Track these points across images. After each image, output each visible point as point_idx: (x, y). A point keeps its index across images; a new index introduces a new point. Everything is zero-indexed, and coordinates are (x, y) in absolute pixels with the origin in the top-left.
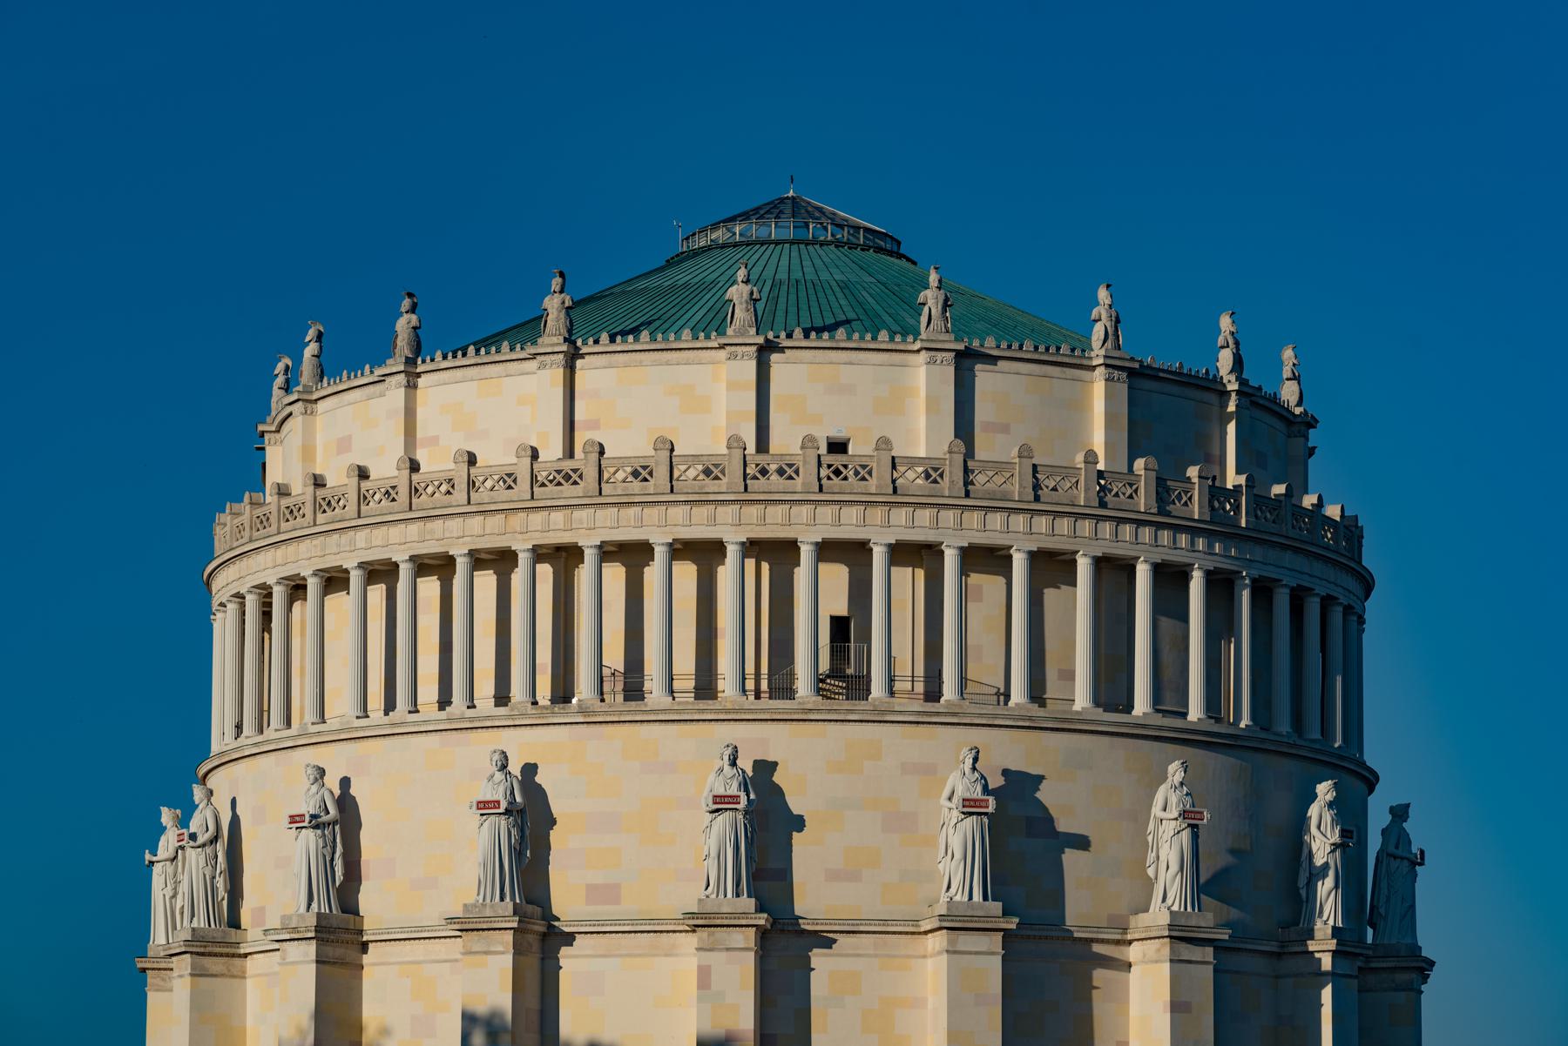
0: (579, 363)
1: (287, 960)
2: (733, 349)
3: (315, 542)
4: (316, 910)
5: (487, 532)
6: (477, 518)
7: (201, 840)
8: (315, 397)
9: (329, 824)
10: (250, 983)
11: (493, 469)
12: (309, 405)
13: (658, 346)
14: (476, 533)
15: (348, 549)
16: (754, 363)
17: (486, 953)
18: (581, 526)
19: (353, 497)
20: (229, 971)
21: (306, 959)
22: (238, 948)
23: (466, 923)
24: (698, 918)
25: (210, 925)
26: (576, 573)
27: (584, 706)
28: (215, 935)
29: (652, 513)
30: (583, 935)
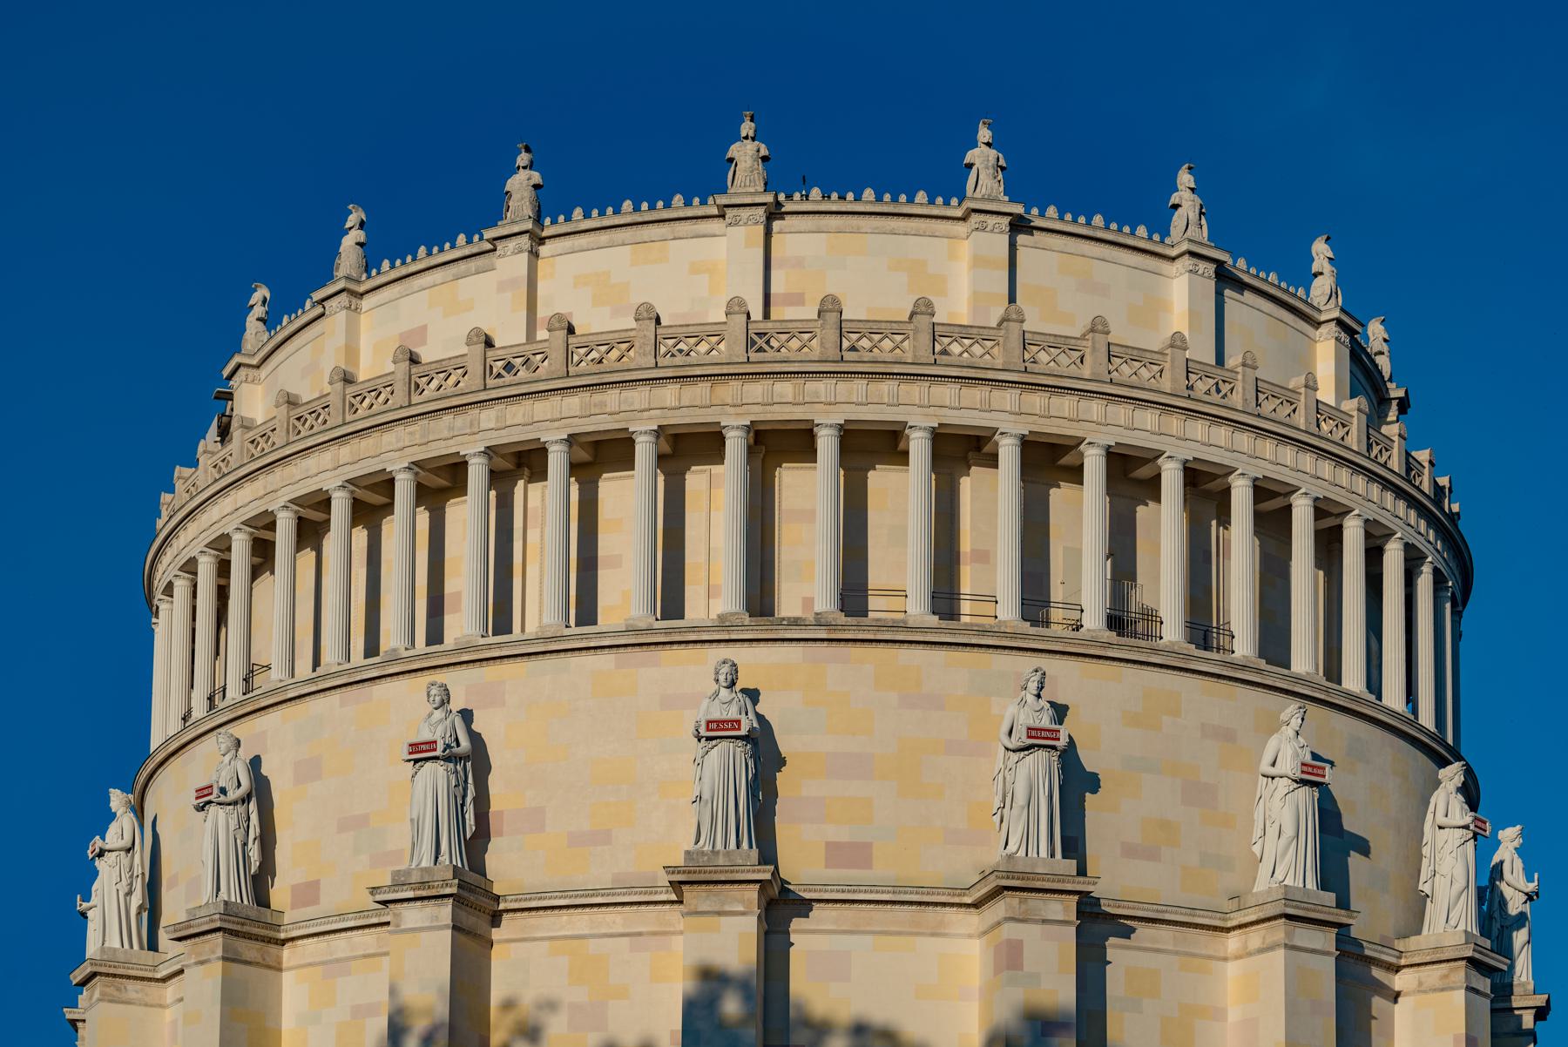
0: (777, 225)
1: (403, 927)
2: (982, 217)
3: (409, 429)
4: (447, 862)
5: (685, 402)
6: (670, 386)
7: (233, 795)
8: (362, 289)
9: (461, 759)
10: (285, 974)
11: (691, 329)
12: (354, 300)
13: (885, 209)
14: (668, 404)
15: (468, 431)
16: (1006, 237)
17: (719, 913)
18: (817, 400)
19: (476, 368)
20: (264, 959)
21: (435, 924)
22: (279, 931)
23: (695, 872)
24: (1013, 878)
25: (242, 901)
26: (777, 473)
27: (822, 620)
28: (249, 913)
29: (915, 391)
30: (822, 905)
